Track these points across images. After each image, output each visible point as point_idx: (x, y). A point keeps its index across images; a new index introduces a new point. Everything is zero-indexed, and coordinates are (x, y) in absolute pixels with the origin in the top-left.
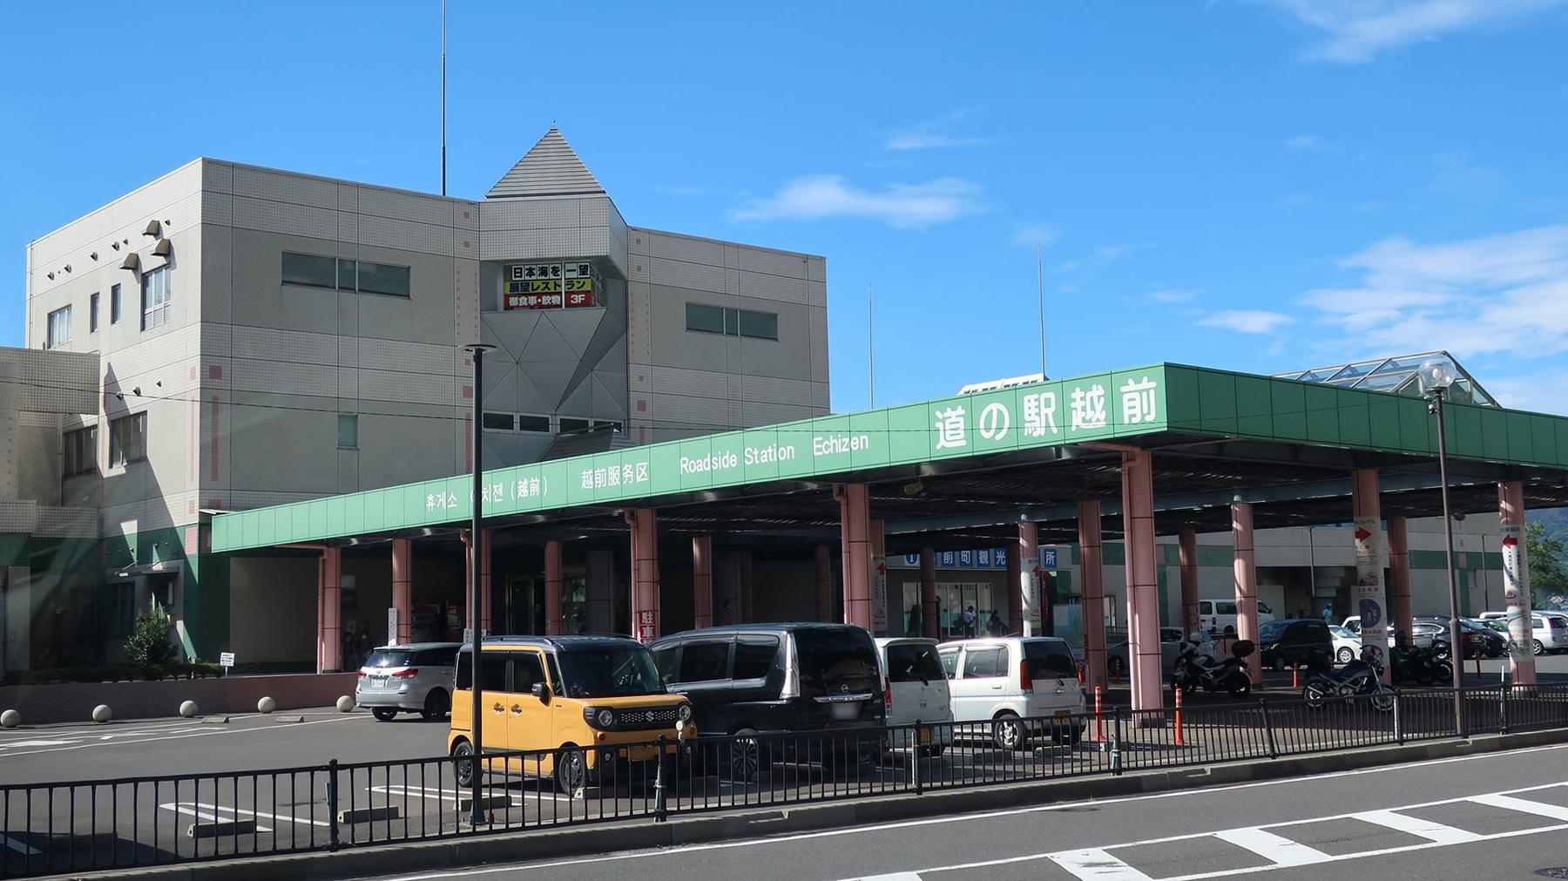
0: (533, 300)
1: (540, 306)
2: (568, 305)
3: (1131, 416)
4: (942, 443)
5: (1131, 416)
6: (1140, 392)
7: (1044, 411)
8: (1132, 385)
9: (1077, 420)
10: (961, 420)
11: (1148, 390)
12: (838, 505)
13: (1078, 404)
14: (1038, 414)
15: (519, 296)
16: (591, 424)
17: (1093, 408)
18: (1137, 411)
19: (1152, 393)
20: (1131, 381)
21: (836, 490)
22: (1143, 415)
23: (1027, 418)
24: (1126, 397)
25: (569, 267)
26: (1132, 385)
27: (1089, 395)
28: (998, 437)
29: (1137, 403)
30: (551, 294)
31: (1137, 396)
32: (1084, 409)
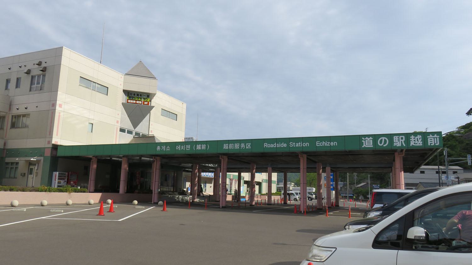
0: (134, 102)
1: (136, 103)
2: (143, 104)
3: (430, 144)
4: (364, 145)
5: (430, 144)
6: (434, 138)
7: (400, 140)
8: (231, 144)
9: (412, 143)
10: (371, 141)
11: (436, 138)
12: (221, 160)
13: (413, 139)
14: (399, 141)
15: (131, 100)
16: (141, 135)
17: (418, 141)
18: (433, 142)
19: (438, 139)
20: (418, 136)
21: (220, 157)
22: (435, 144)
23: (395, 142)
24: (429, 139)
25: (144, 95)
26: (231, 144)
27: (416, 137)
28: (384, 146)
29: (433, 140)
30: (139, 101)
31: (433, 139)
32: (415, 141)
